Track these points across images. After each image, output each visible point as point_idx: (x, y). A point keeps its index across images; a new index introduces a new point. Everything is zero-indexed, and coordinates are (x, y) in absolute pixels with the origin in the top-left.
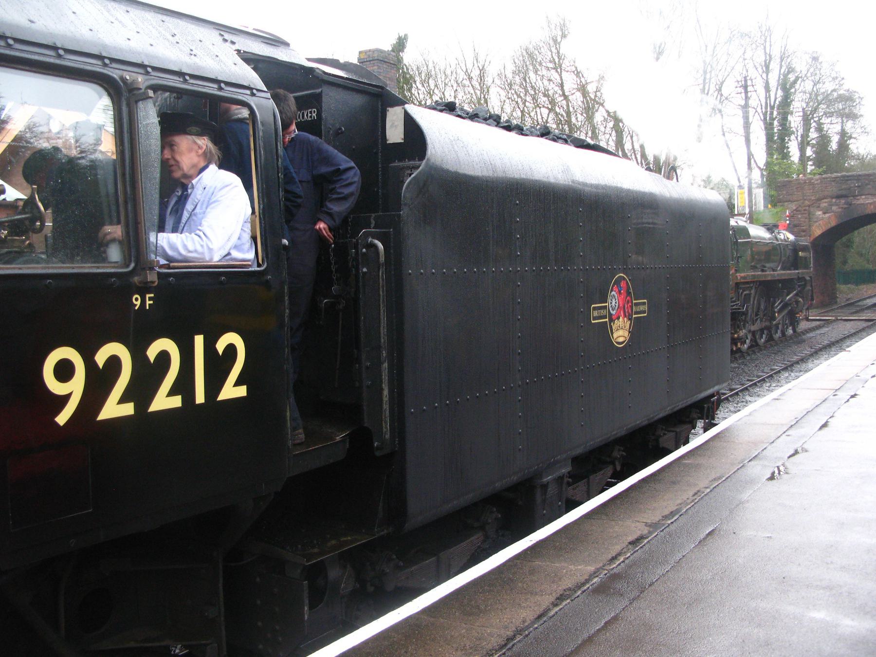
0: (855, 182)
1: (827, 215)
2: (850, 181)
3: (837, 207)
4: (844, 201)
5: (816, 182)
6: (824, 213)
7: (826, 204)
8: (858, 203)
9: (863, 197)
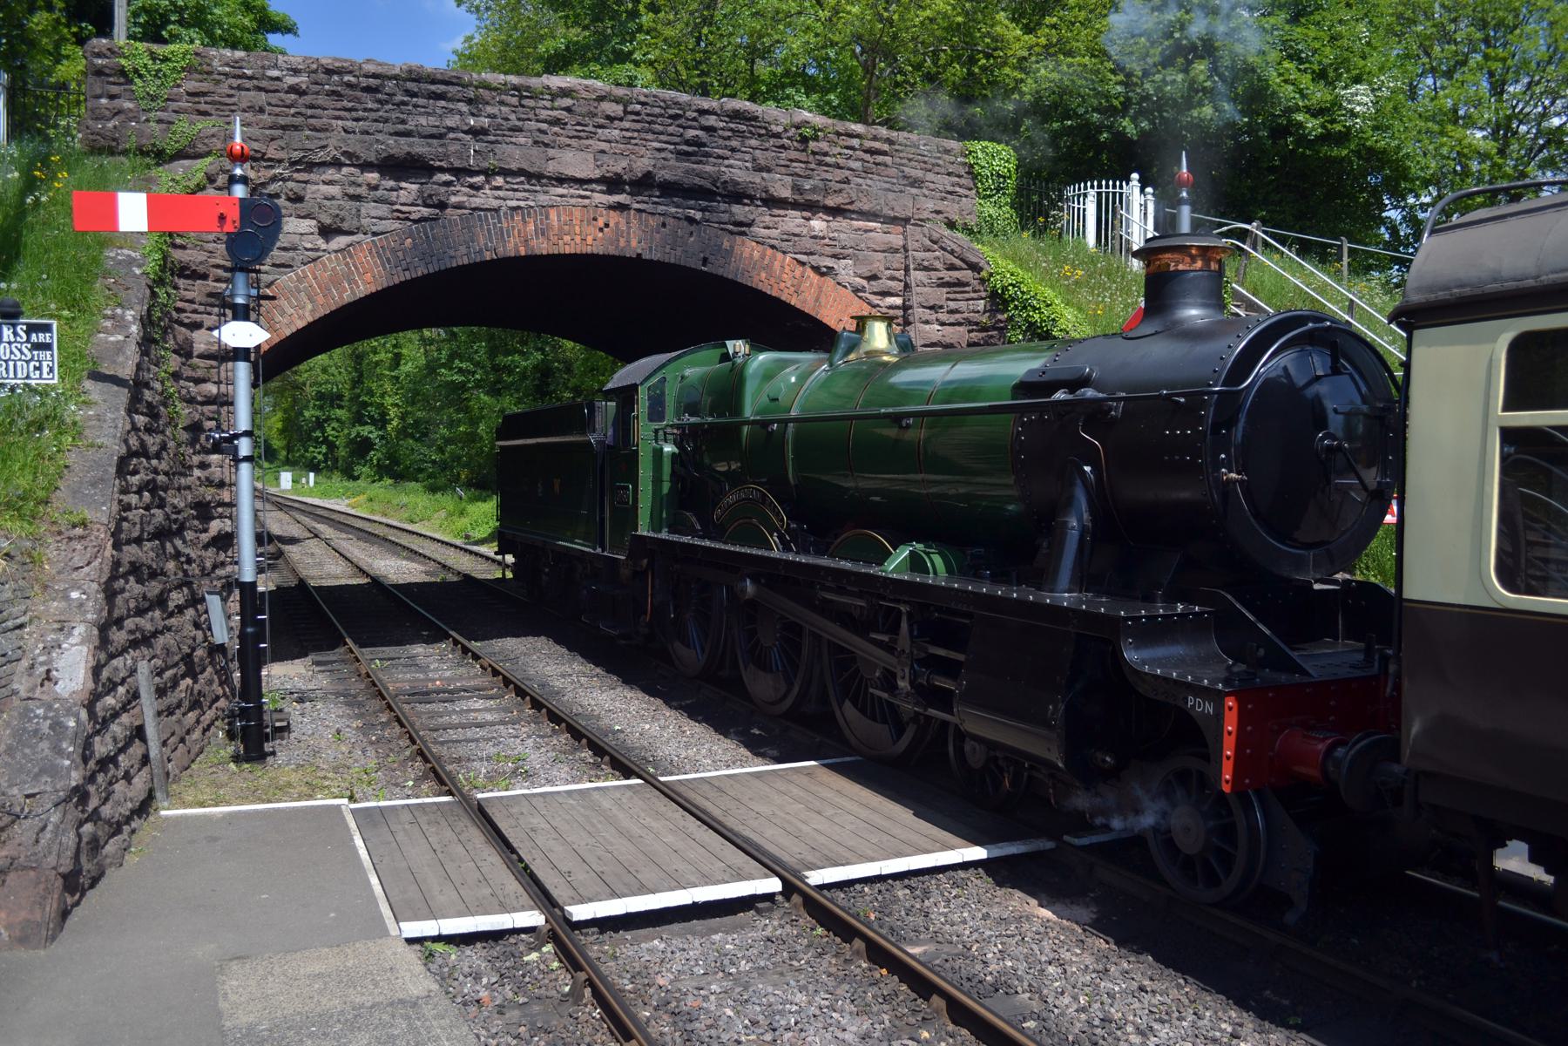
0: (463, 107)
1: (340, 241)
2: (443, 103)
3: (383, 210)
4: (415, 187)
5: (291, 80)
6: (327, 232)
7: (334, 190)
8: (477, 202)
9: (499, 181)
